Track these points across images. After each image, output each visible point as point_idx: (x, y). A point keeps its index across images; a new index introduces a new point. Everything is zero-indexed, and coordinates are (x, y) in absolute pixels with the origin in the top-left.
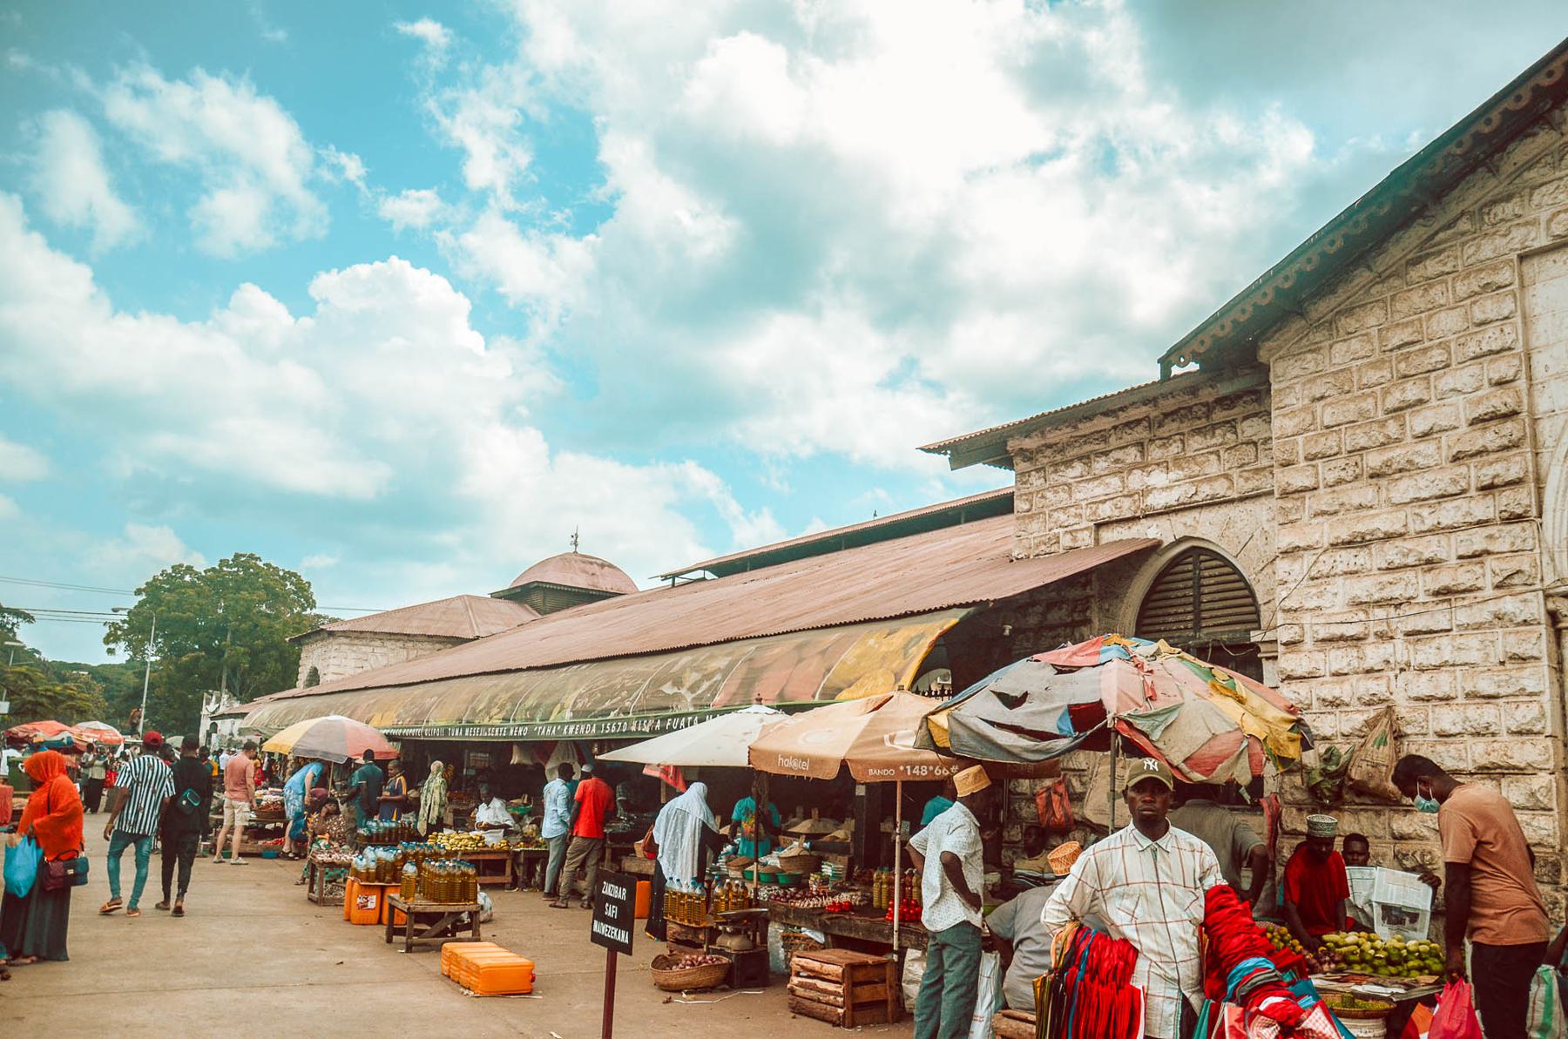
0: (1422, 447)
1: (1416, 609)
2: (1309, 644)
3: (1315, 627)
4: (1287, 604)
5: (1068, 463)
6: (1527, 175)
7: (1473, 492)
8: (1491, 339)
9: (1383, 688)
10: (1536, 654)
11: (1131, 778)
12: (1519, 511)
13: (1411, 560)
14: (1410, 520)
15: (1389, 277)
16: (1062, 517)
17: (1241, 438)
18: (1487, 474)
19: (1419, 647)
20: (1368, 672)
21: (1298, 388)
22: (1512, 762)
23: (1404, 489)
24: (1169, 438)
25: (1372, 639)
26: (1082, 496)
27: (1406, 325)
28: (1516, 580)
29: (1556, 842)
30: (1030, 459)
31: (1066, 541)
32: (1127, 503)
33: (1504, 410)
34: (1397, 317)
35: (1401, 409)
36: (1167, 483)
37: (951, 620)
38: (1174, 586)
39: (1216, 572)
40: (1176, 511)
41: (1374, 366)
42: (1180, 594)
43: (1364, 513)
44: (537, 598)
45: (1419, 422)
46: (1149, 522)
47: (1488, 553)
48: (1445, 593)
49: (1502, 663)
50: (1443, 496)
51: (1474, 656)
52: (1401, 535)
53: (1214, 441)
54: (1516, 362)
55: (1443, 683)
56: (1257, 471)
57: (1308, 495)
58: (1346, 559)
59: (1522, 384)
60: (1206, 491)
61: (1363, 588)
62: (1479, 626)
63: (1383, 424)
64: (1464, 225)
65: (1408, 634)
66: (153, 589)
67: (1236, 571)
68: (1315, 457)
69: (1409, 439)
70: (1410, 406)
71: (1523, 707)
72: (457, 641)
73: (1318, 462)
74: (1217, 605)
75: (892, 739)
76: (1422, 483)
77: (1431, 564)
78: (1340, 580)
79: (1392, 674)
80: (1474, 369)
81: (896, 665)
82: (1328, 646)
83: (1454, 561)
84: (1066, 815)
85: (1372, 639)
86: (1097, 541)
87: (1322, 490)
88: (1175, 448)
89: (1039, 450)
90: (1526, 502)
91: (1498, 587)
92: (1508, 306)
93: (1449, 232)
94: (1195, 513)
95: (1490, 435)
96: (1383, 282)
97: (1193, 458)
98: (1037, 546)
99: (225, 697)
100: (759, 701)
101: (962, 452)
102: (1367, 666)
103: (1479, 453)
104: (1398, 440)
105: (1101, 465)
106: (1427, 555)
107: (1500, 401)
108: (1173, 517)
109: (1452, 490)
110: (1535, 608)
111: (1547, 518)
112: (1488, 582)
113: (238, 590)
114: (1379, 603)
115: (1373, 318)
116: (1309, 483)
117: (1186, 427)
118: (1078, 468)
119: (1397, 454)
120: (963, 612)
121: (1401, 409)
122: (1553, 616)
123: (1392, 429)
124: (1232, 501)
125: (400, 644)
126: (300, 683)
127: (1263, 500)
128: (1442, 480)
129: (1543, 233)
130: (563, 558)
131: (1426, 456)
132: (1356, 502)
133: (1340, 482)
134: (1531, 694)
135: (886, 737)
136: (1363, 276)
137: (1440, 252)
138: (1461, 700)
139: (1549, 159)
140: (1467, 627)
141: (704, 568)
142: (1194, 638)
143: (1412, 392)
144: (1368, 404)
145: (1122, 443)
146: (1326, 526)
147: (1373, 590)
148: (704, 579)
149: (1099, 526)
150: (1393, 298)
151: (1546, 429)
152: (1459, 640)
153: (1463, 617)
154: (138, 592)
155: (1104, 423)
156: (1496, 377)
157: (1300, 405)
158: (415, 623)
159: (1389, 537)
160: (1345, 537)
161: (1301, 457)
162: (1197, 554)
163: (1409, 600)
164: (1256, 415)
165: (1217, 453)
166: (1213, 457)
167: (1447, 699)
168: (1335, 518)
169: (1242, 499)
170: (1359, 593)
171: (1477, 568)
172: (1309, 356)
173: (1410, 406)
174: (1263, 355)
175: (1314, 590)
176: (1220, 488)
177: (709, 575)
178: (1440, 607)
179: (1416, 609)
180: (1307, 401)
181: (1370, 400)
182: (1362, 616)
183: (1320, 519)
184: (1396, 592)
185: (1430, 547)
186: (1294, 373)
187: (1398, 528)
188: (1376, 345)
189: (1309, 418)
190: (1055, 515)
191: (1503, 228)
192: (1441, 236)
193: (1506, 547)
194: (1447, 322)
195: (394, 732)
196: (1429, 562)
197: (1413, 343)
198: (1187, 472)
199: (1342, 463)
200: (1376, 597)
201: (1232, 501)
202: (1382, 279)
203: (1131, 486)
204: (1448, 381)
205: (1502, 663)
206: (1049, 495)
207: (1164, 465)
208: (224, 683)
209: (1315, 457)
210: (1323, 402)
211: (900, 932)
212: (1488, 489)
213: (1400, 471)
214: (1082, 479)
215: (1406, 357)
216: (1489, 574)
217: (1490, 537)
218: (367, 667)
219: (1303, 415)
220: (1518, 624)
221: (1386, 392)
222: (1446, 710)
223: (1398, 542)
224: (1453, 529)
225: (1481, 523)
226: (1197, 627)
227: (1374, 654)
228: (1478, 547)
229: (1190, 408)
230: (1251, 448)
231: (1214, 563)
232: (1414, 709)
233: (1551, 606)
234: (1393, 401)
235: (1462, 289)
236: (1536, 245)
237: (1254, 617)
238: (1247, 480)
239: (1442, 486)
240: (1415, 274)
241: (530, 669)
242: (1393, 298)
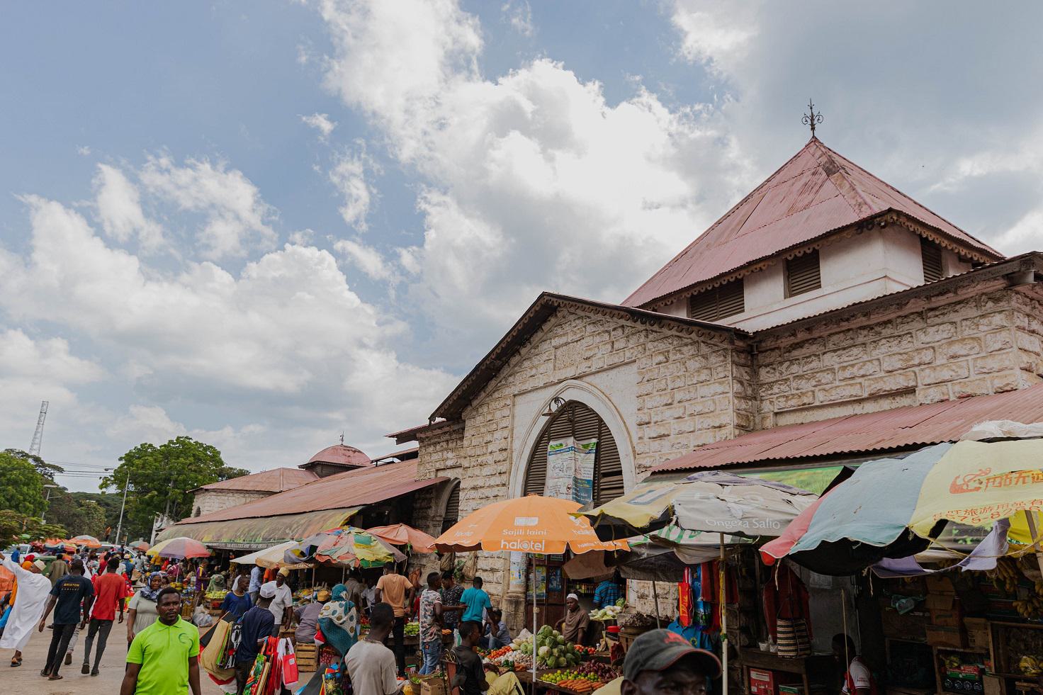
23: (486, 471)
37: (361, 507)
44: (319, 469)
66: (129, 458)
72: (272, 493)
78: (471, 501)
86: (436, 476)
98: (421, 477)
99: (165, 518)
100: (293, 539)
101: (401, 438)
108: (454, 470)
113: (178, 457)
125: (242, 495)
126: (192, 515)
130: (334, 448)
141: (393, 457)
148: (393, 462)
149: (437, 470)
154: (121, 459)
158: (251, 484)
177: (396, 460)
195: (210, 544)
202: (488, 396)
207: (452, 450)
208: (167, 510)
218: (225, 507)
241: (261, 517)
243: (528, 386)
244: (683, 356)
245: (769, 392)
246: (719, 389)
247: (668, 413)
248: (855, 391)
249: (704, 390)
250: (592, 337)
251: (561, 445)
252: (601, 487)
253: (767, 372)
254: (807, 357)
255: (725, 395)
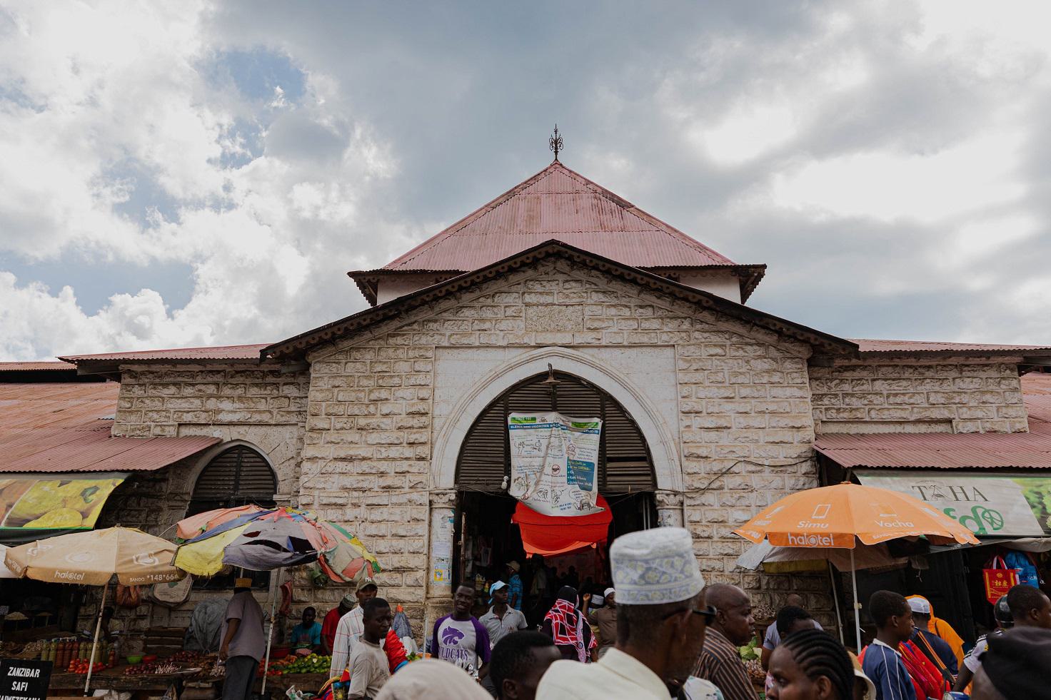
0: (384, 420)
1: (374, 494)
2: (316, 505)
3: (319, 497)
4: (307, 485)
5: (165, 385)
6: (444, 314)
7: (405, 444)
8: (421, 379)
9: (354, 530)
10: (423, 518)
11: (360, 586)
12: (424, 456)
13: (374, 471)
14: (375, 452)
15: (379, 338)
16: (155, 416)
17: (281, 394)
18: (412, 438)
19: (372, 511)
20: (346, 522)
21: (326, 379)
22: (410, 566)
23: (374, 438)
24: (237, 384)
25: (349, 506)
26: (172, 406)
27: (385, 363)
28: (419, 486)
29: (423, 600)
30: (135, 377)
31: (158, 431)
32: (204, 415)
33: (423, 411)
34: (380, 358)
35: (377, 401)
36: (232, 409)
38: (224, 464)
39: (252, 460)
40: (235, 425)
41: (366, 377)
42: (228, 469)
43: (353, 445)
45: (385, 409)
46: (216, 427)
47: (408, 472)
48: (387, 488)
49: (409, 522)
50: (391, 444)
51: (397, 518)
52: (370, 459)
53: (265, 392)
54: (430, 392)
55: (383, 529)
56: (289, 412)
57: (324, 432)
58: (341, 466)
59: (430, 401)
60: (257, 418)
61: (348, 481)
62: (401, 504)
63: (368, 406)
64: (415, 326)
65: (368, 505)
67: (268, 465)
68: (331, 414)
69: (378, 415)
70: (381, 400)
71: (416, 541)
73: (333, 417)
74: (250, 478)
75: (137, 559)
76: (383, 436)
77: (382, 474)
79: (358, 524)
80: (412, 390)
81: (81, 505)
82: (326, 508)
83: (393, 474)
84: (138, 596)
85: (349, 506)
87: (332, 431)
88: (240, 391)
89: (143, 373)
90: (427, 452)
91: (411, 488)
92: (429, 367)
93: (410, 327)
94: (246, 428)
95: (416, 421)
96: (376, 340)
97: (251, 398)
102: (346, 519)
103: (410, 428)
104: (374, 415)
105: (188, 391)
106: (382, 470)
107: (421, 407)
109: (396, 442)
110: (426, 500)
111: (434, 459)
112: (407, 485)
114: (355, 489)
115: (369, 356)
116: (326, 426)
117: (248, 381)
118: (172, 390)
119: (373, 421)
120: (125, 476)
121: (377, 401)
122: (431, 502)
123: (372, 409)
124: (270, 425)
127: (288, 427)
128: (393, 436)
129: (446, 340)
131: (386, 425)
132: (350, 440)
133: (342, 429)
134: (420, 536)
135: (134, 557)
136: (368, 335)
137: (404, 335)
138: (389, 537)
139: (452, 310)
140: (396, 504)
142: (233, 494)
143: (384, 394)
144: (362, 395)
145: (205, 381)
146: (332, 449)
147: (354, 483)
150: (379, 349)
151: (438, 423)
152: (391, 510)
153: (394, 499)
155: (197, 368)
156: (421, 396)
157: (326, 387)
159: (364, 459)
160: (343, 456)
161: (324, 412)
162: (242, 450)
163: (370, 490)
164: (292, 384)
165: (266, 398)
166: (263, 400)
167: (383, 536)
168: (337, 446)
169: (275, 425)
170: (346, 483)
171: (403, 478)
172: (334, 365)
173: (381, 400)
174: (310, 359)
175: (323, 480)
176: (266, 418)
178: (384, 494)
179: (374, 494)
180: (329, 386)
181: (363, 393)
182: (346, 494)
183: (330, 445)
184: (365, 485)
185: (383, 466)
186: (325, 371)
187: (369, 455)
188: (368, 368)
189: (331, 395)
190: (151, 414)
191: (431, 333)
192: (405, 328)
193: (416, 471)
194: (403, 367)
196: (382, 473)
197: (386, 372)
198: (246, 405)
199: (345, 420)
200: (354, 486)
201: (270, 425)
203: (208, 407)
204: (400, 393)
205: (409, 522)
206: (147, 401)
209: (331, 414)
210: (338, 389)
211: (91, 680)
212: (411, 444)
213: (373, 429)
214: (172, 397)
215: (383, 377)
216: (408, 481)
217: (410, 465)
219: (328, 393)
220: (418, 505)
221: (371, 391)
222: (382, 541)
223: (369, 462)
224: (394, 459)
225: (407, 459)
226: (236, 488)
227: (350, 513)
228: (405, 469)
229: (253, 371)
230: (287, 400)
231: (258, 460)
232: (367, 540)
233: (431, 498)
234: (373, 396)
235: (411, 354)
236: (443, 345)
237: (272, 486)
238: (282, 416)
239: (392, 439)
240: (391, 341)
242: (379, 349)
243: (474, 340)
244: (747, 354)
245: (820, 403)
246: (798, 393)
247: (728, 406)
248: (898, 414)
249: (777, 391)
250: (600, 307)
251: (534, 419)
252: (608, 473)
253: (818, 385)
254: (857, 380)
255: (802, 400)
